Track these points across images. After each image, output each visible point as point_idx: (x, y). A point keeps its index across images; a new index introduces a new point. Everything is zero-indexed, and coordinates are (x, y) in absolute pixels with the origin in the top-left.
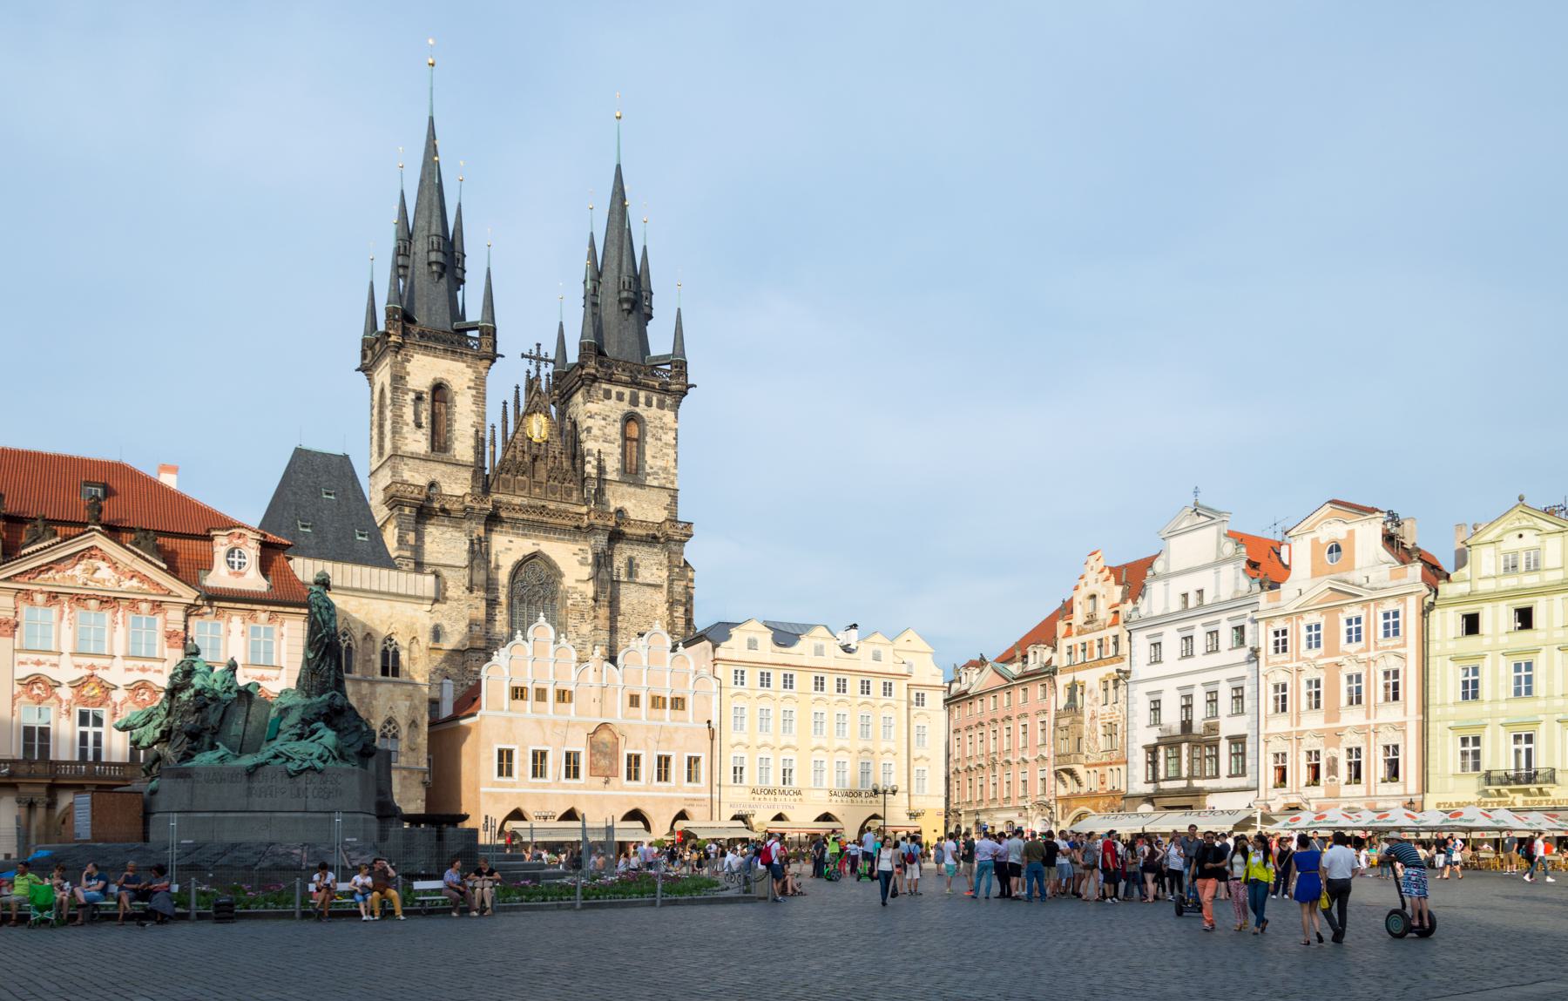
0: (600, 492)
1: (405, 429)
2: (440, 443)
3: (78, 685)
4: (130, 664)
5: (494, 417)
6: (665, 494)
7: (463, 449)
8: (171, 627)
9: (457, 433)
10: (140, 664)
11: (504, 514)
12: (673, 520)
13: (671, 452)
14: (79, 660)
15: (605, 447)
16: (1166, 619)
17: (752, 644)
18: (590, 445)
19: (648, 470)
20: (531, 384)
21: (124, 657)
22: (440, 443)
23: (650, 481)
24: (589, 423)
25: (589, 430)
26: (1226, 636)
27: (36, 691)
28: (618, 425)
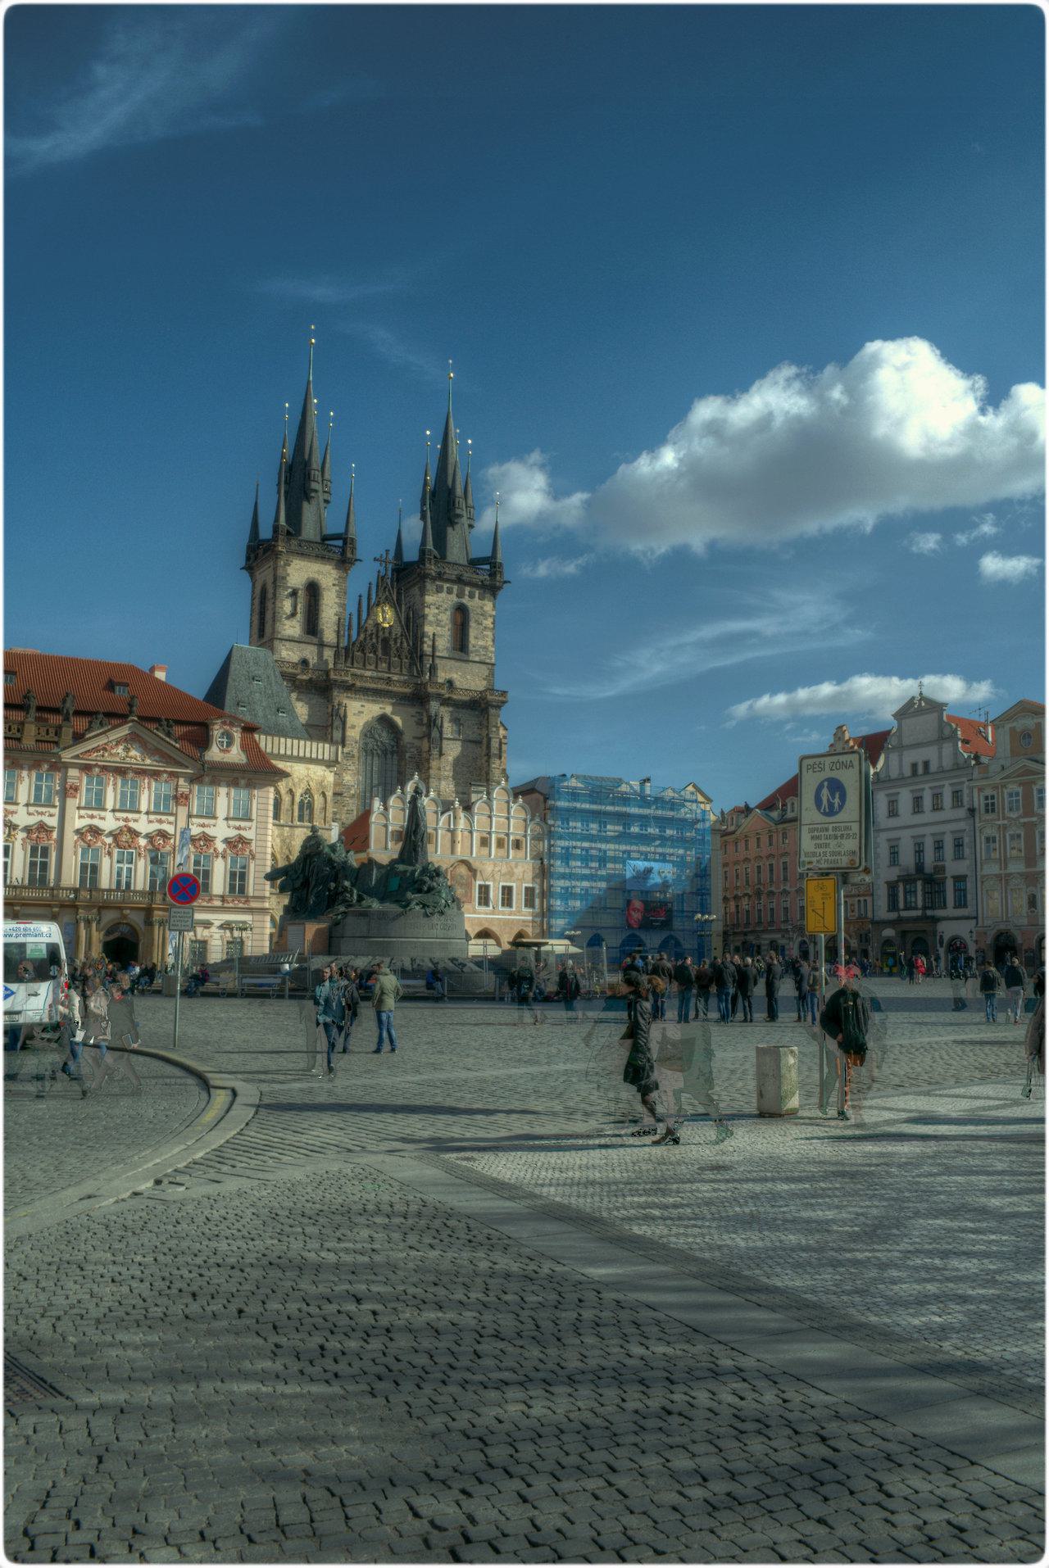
0: (433, 669)
2: (312, 626)
5: (352, 609)
11: (358, 684)
12: (491, 689)
13: (489, 634)
14: (118, 815)
16: (901, 780)
18: (429, 629)
19: (471, 648)
24: (427, 611)
25: (424, 617)
26: (947, 800)
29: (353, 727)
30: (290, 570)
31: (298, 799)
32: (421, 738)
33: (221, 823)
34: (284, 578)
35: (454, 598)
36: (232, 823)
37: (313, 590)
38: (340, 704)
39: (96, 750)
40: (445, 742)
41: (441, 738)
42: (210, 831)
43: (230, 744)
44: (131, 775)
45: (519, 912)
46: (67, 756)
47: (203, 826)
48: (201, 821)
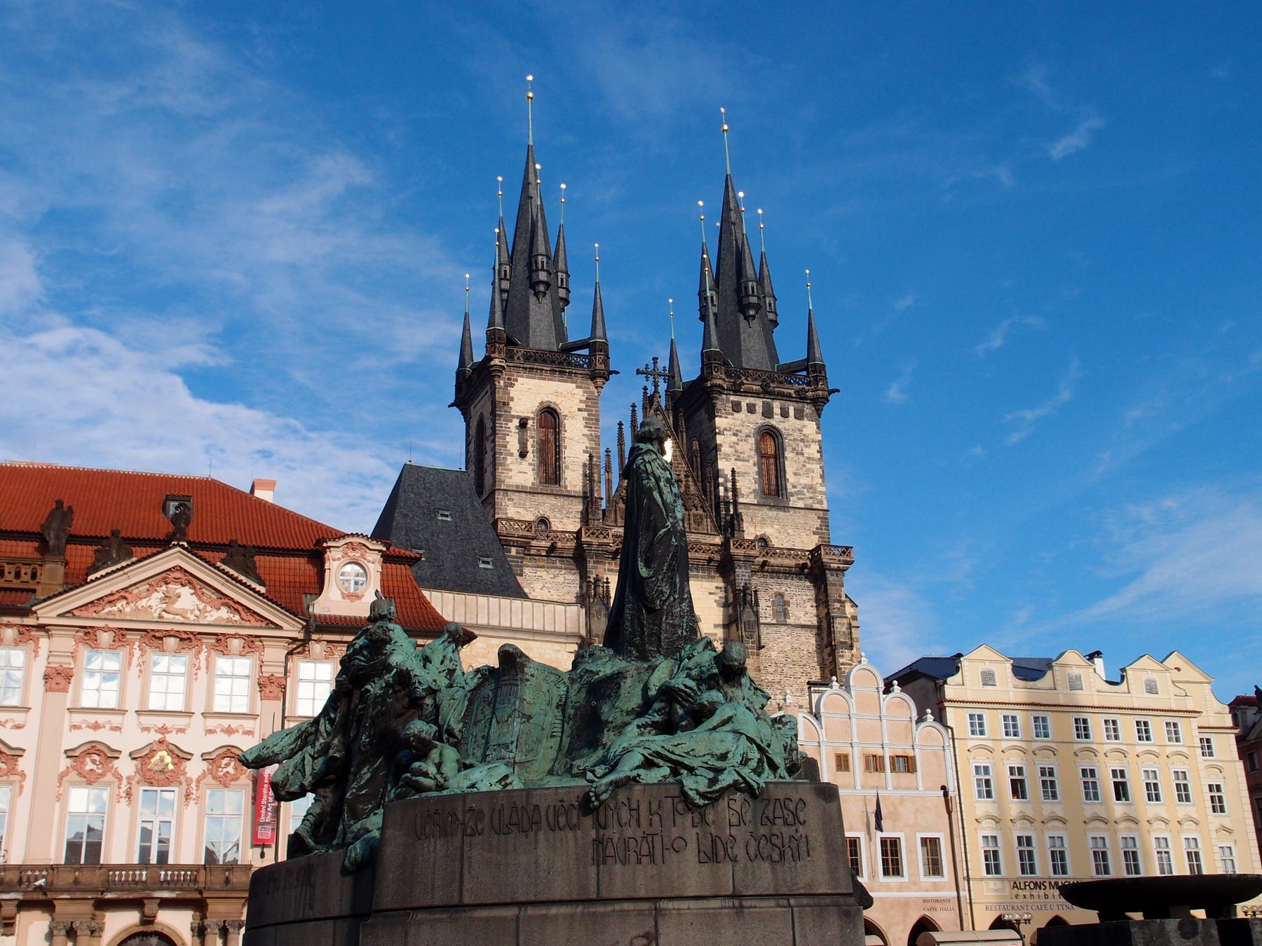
0: (737, 517)
1: (509, 460)
2: (551, 472)
3: (142, 757)
4: (212, 723)
6: (813, 515)
7: (573, 479)
10: (225, 723)
13: (816, 467)
14: (147, 721)
15: (739, 466)
17: (988, 679)
18: (724, 465)
19: (790, 489)
20: (649, 401)
22: (551, 472)
23: (793, 501)
24: (719, 439)
25: (716, 448)
27: (90, 766)
28: (752, 440)
30: (513, 392)
37: (550, 416)
38: (597, 580)
39: (110, 599)
40: (763, 630)
41: (758, 623)
44: (171, 642)
45: (915, 883)
46: (47, 613)
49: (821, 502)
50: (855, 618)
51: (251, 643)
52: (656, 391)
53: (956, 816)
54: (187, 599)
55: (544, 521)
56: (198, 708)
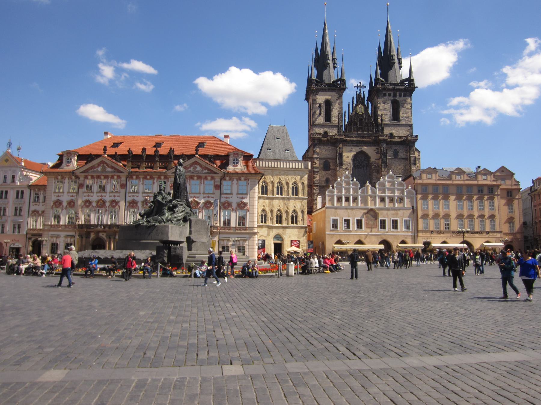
0: (382, 130)
4: (205, 195)
5: (345, 108)
7: (335, 120)
8: (122, 182)
9: (333, 115)
10: (208, 195)
13: (410, 111)
18: (380, 113)
21: (204, 193)
25: (378, 107)
28: (389, 105)
29: (348, 157)
31: (291, 186)
32: (379, 159)
33: (235, 196)
34: (315, 100)
35: (392, 98)
36: (239, 196)
42: (230, 200)
43: (237, 163)
47: (227, 198)
48: (226, 196)
49: (411, 122)
50: (419, 155)
51: (212, 178)
52: (360, 92)
53: (415, 213)
54: (199, 168)
55: (326, 133)
56: (202, 192)
